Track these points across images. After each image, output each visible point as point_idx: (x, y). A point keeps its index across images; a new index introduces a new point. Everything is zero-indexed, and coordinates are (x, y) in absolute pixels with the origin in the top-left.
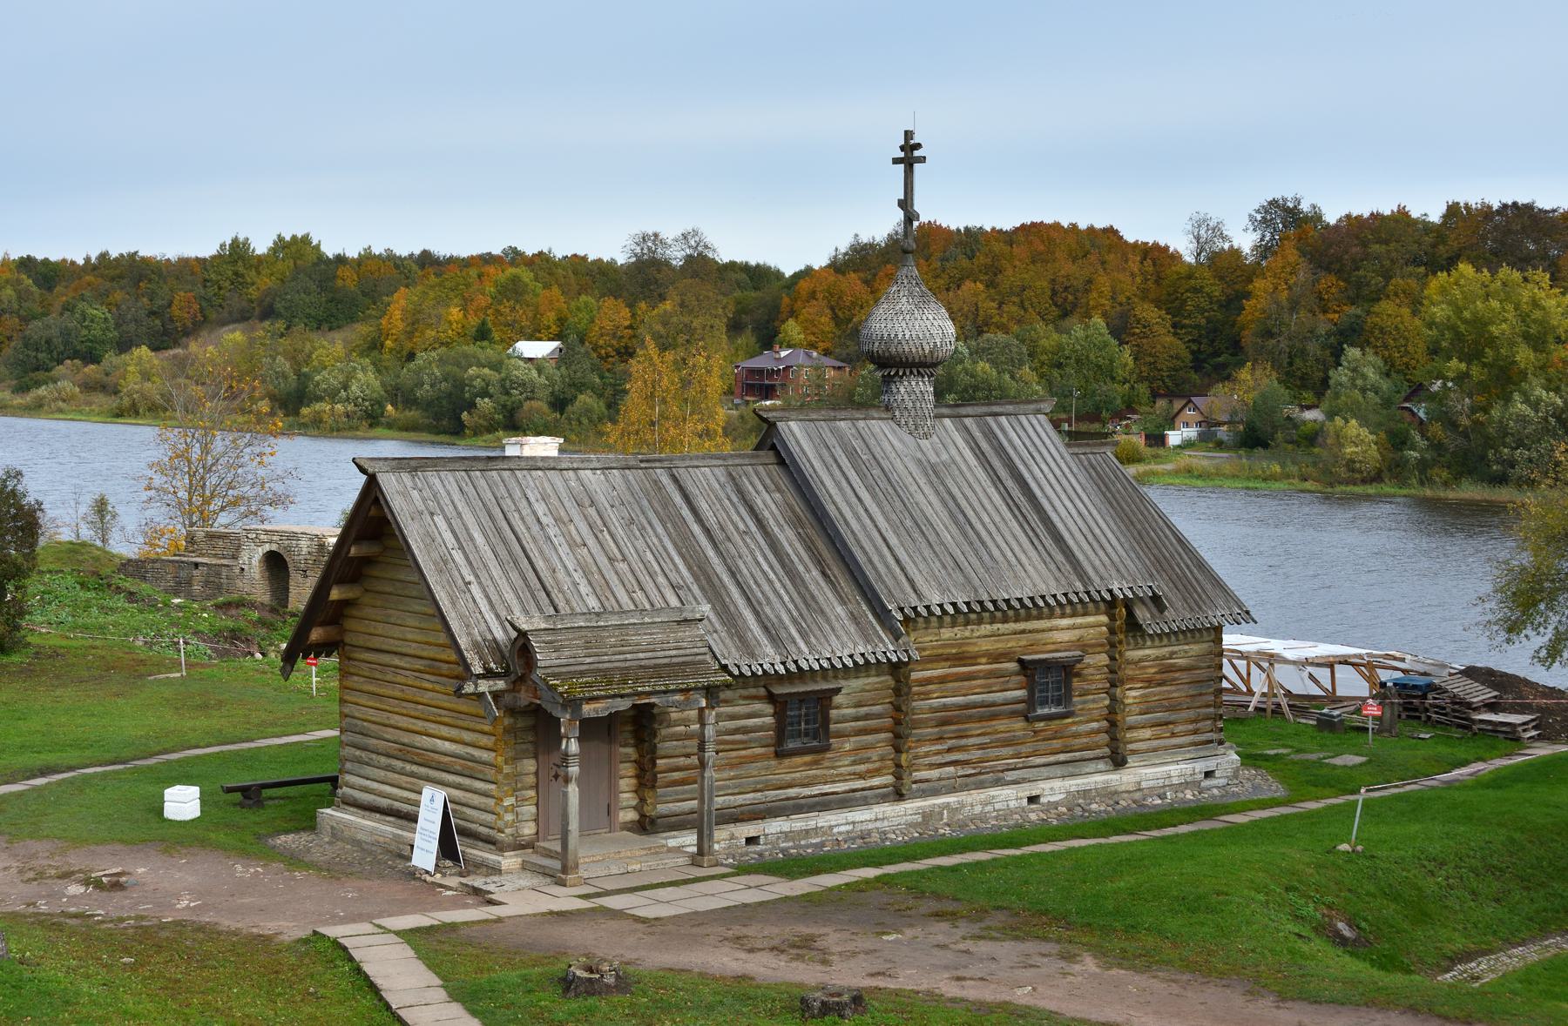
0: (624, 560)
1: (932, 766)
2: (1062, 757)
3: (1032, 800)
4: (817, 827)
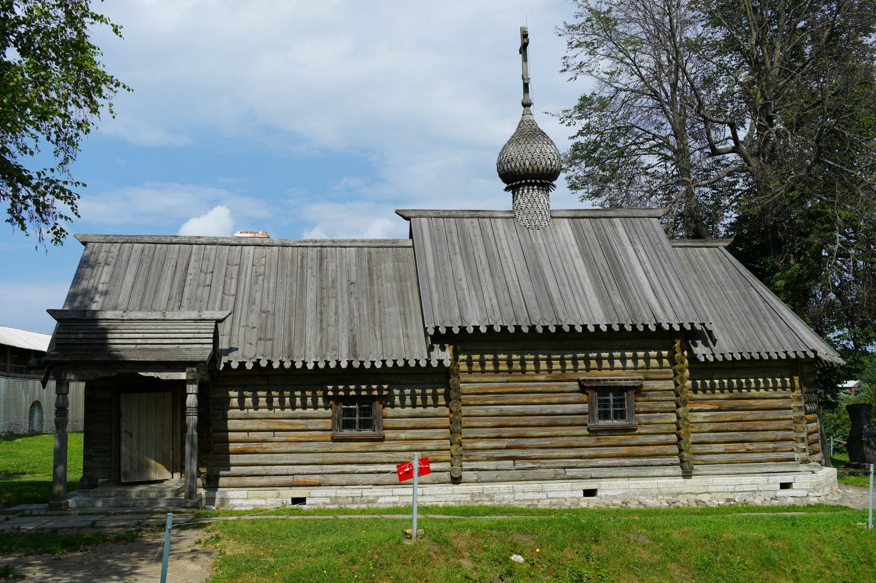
0: (236, 295)
1: (489, 459)
2: (627, 461)
3: (590, 493)
4: (362, 496)
